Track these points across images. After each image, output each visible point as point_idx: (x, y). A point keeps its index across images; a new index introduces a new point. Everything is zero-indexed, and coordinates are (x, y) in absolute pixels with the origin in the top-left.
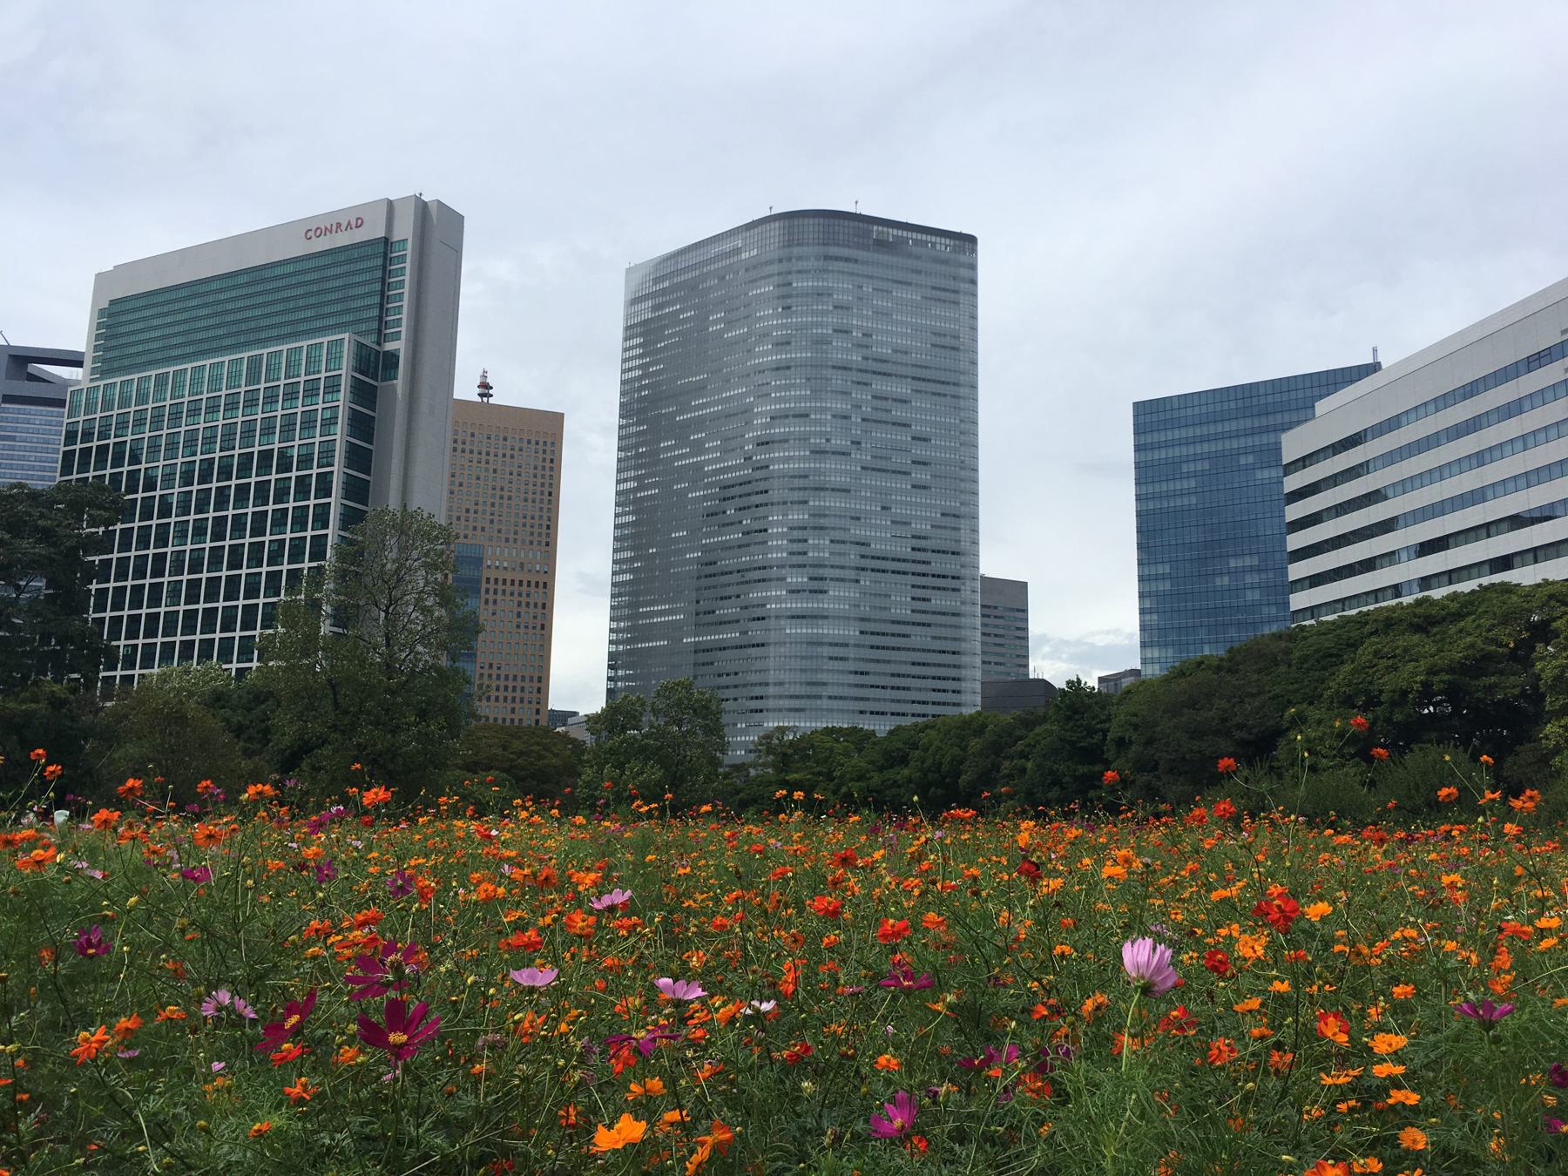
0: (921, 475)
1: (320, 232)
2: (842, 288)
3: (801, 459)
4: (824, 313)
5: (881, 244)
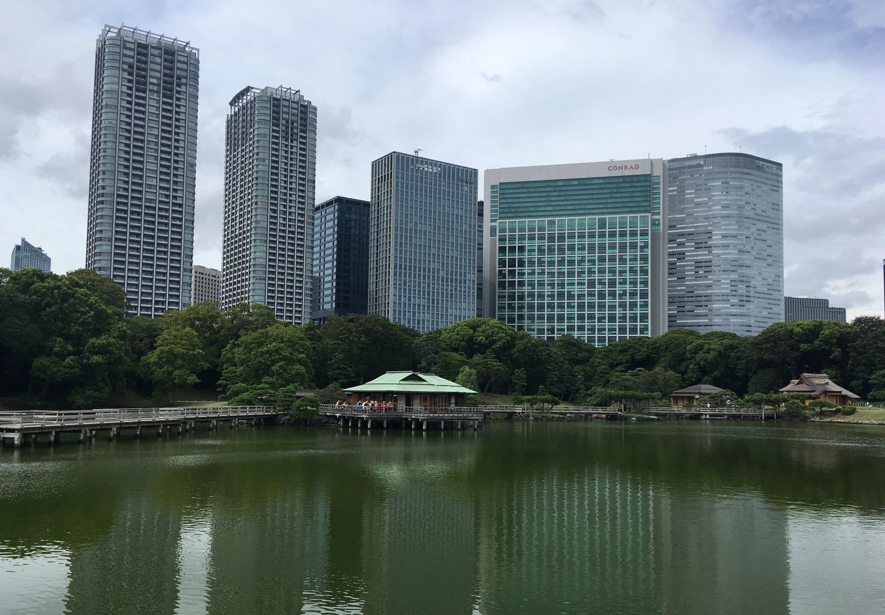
0: (770, 260)
1: (615, 168)
2: (747, 184)
3: (735, 254)
4: (741, 196)
5: (759, 168)
